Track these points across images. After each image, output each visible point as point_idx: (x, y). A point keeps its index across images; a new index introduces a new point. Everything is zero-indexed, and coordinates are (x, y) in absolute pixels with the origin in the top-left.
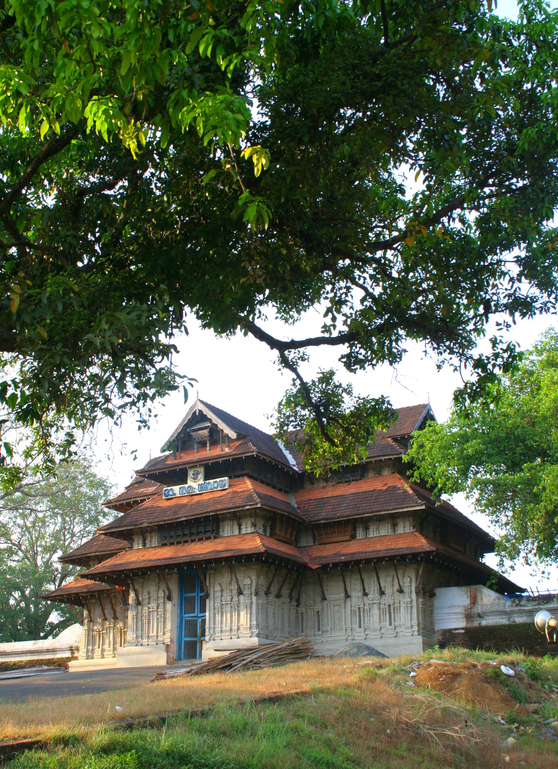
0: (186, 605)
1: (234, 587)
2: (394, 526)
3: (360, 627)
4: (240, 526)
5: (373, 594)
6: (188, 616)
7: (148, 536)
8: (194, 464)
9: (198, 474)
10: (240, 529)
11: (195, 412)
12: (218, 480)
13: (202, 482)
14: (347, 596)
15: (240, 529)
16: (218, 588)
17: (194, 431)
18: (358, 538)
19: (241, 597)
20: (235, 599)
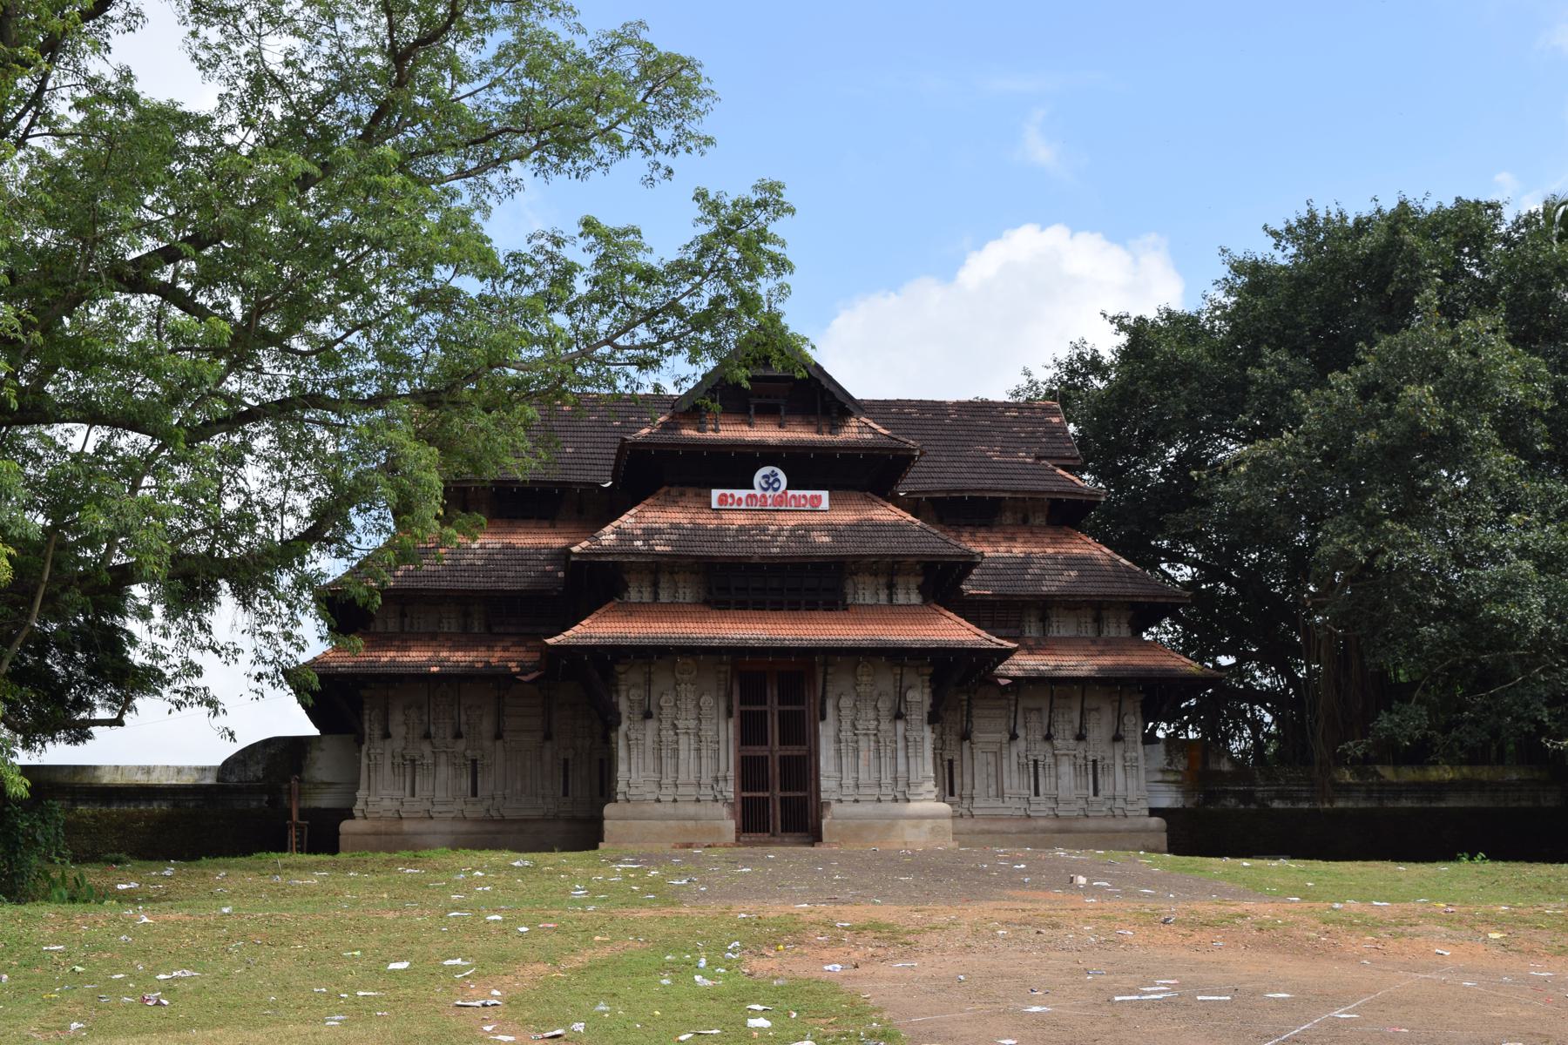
0: (751, 731)
1: (885, 705)
2: (1098, 621)
3: (1037, 794)
5: (1065, 741)
16: (846, 702)
19: (900, 725)
20: (885, 725)
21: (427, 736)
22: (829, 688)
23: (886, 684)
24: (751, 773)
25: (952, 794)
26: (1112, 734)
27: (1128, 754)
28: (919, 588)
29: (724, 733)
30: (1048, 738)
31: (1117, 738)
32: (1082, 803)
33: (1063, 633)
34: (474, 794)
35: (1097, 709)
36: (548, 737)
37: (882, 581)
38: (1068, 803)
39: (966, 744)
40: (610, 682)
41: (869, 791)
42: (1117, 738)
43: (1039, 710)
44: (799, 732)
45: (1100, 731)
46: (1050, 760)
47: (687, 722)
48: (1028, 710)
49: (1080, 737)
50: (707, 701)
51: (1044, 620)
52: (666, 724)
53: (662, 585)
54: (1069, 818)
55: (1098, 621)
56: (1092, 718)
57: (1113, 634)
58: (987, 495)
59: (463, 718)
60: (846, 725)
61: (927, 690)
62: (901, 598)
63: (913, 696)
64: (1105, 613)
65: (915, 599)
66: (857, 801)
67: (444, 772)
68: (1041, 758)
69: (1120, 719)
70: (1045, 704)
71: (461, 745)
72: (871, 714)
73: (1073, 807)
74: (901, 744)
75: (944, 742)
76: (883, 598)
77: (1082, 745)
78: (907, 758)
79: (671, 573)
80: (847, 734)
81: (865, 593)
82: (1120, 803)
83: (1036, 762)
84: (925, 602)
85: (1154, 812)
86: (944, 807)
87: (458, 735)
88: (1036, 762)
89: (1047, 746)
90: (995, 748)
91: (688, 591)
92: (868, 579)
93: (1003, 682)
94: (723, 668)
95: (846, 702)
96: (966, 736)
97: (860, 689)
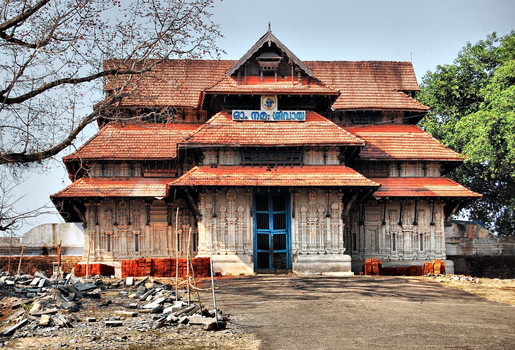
0: (261, 222)
1: (321, 210)
2: (425, 169)
3: (394, 249)
4: (325, 157)
5: (407, 224)
6: (261, 231)
7: (221, 153)
8: (269, 94)
9: (272, 102)
10: (325, 160)
11: (267, 43)
12: (296, 112)
13: (276, 110)
14: (384, 223)
15: (325, 160)
16: (304, 209)
17: (262, 60)
18: (391, 176)
21: (116, 224)
22: (296, 203)
23: (322, 202)
24: (261, 241)
25: (355, 249)
26: (430, 222)
27: (437, 231)
28: (337, 157)
29: (250, 223)
30: (400, 224)
31: (432, 224)
32: (415, 254)
33: (408, 175)
34: (137, 250)
35: (423, 210)
36: (170, 224)
37: (321, 154)
38: (408, 253)
39: (362, 226)
40: (197, 200)
41: (314, 249)
42: (432, 224)
43: (396, 210)
44: (282, 222)
45: (424, 221)
46: (401, 234)
47: (231, 219)
48: (390, 211)
49: (415, 224)
50: (241, 209)
51: (399, 169)
52: (223, 220)
53: (220, 156)
54: (409, 260)
55: (425, 169)
56: (421, 213)
57: (431, 176)
58: (374, 110)
59: (131, 215)
60: (304, 220)
61: (341, 204)
62: (329, 162)
63: (335, 206)
64: (428, 166)
65: (336, 162)
66: (308, 254)
67: (124, 240)
68: (396, 233)
69: (433, 214)
70: (399, 209)
71: (131, 228)
72: (315, 215)
73: (411, 255)
74: (329, 228)
75: (351, 226)
76: (321, 162)
77: (415, 228)
78: (332, 234)
79: (225, 151)
80: (304, 224)
81: (313, 159)
82: (433, 254)
83: (394, 234)
84: (340, 164)
85: (449, 257)
86: (348, 257)
87: (129, 224)
88: (394, 234)
89: (399, 227)
90: (374, 228)
91: (232, 159)
92: (315, 153)
93: (378, 199)
94: (248, 194)
95: (304, 209)
96: (361, 223)
97: (311, 203)
